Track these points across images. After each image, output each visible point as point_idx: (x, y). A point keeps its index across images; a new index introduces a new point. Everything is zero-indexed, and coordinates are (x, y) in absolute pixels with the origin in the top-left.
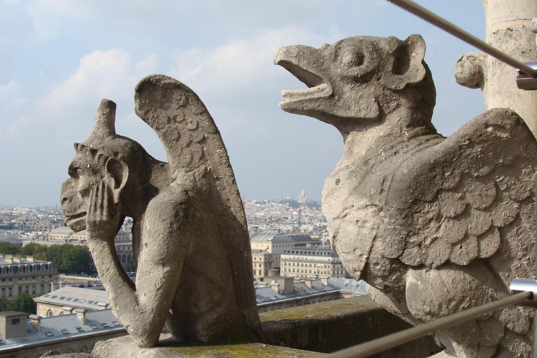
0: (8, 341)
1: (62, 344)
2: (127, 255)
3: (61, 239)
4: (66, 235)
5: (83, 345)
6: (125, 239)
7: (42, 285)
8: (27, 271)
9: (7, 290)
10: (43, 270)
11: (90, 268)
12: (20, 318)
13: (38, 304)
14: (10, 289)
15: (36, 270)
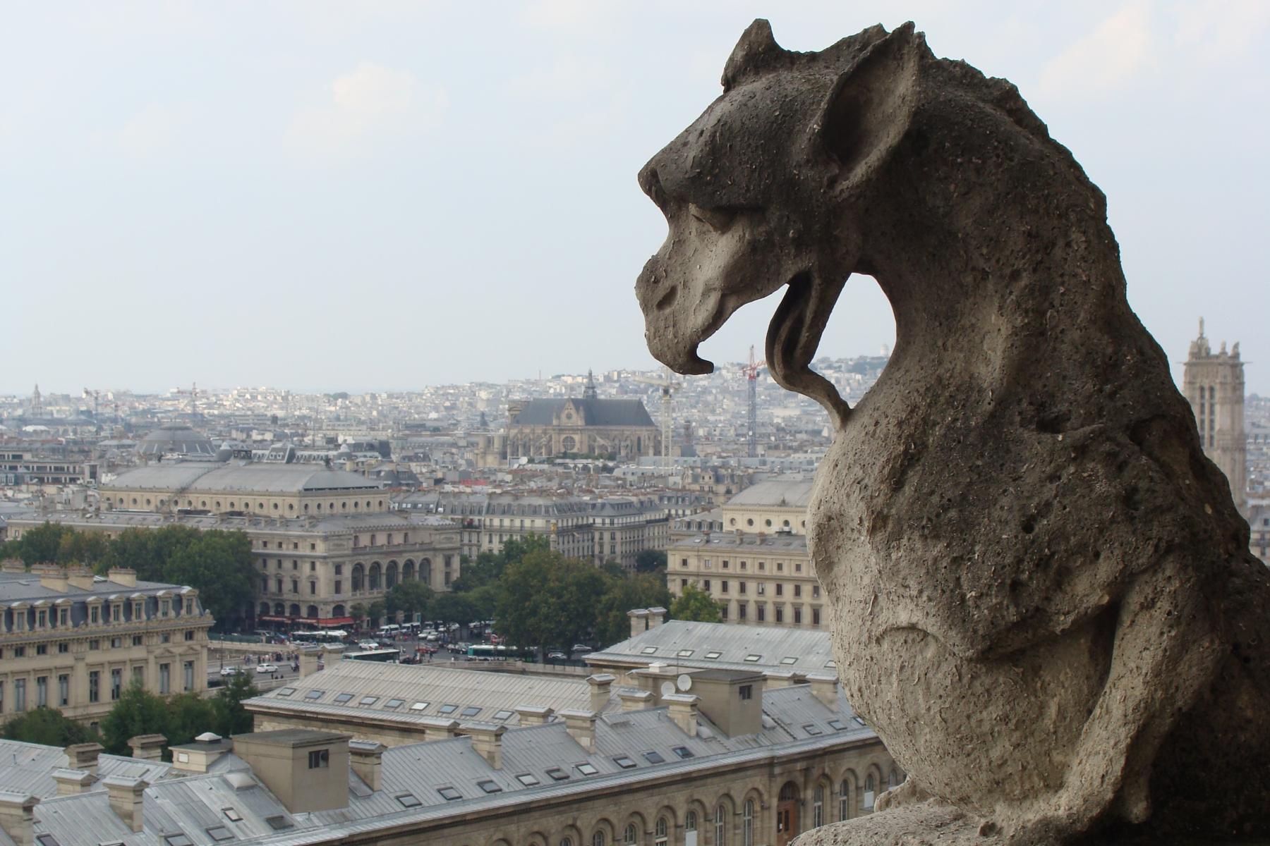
0: (299, 818)
1: (446, 831)
2: (385, 563)
3: (146, 508)
4: (165, 497)
5: (500, 835)
6: (375, 508)
7: (165, 667)
8: (117, 618)
9: (53, 683)
10: (165, 614)
11: (258, 610)
12: (331, 748)
13: (257, 719)
14: (64, 679)
15: (144, 617)
